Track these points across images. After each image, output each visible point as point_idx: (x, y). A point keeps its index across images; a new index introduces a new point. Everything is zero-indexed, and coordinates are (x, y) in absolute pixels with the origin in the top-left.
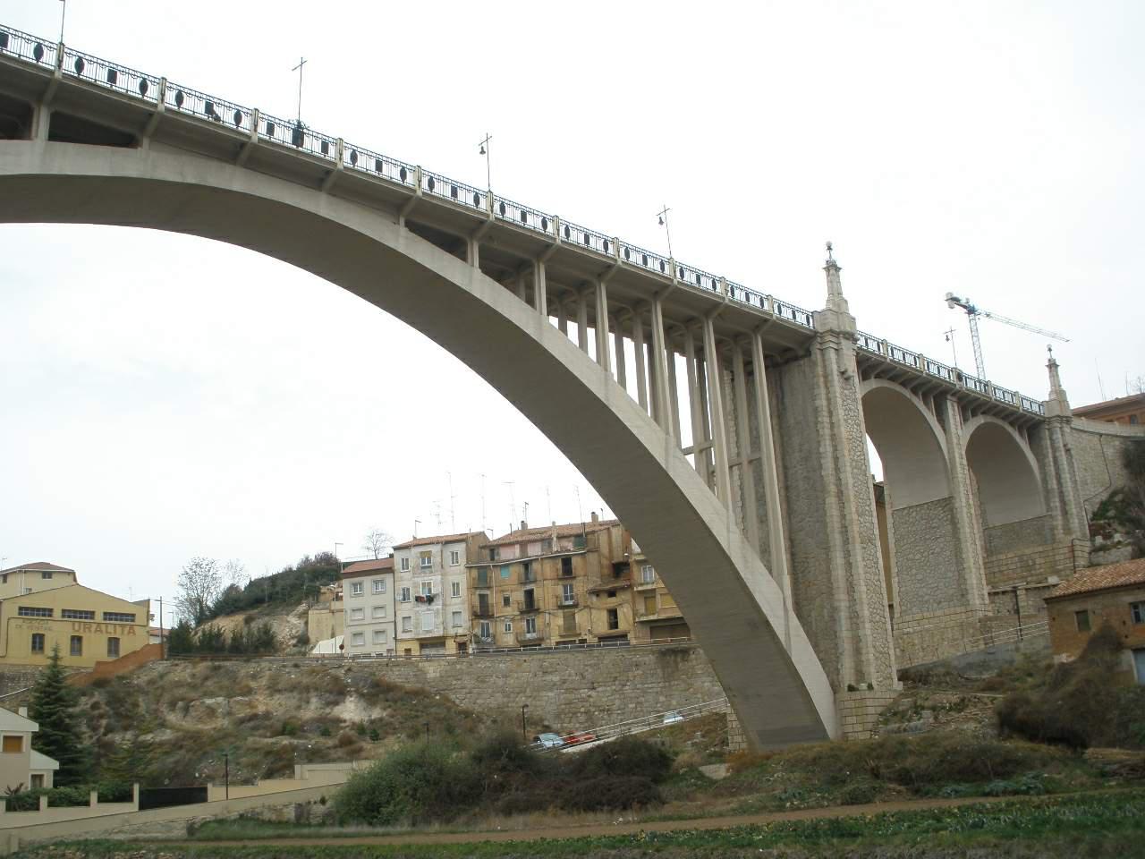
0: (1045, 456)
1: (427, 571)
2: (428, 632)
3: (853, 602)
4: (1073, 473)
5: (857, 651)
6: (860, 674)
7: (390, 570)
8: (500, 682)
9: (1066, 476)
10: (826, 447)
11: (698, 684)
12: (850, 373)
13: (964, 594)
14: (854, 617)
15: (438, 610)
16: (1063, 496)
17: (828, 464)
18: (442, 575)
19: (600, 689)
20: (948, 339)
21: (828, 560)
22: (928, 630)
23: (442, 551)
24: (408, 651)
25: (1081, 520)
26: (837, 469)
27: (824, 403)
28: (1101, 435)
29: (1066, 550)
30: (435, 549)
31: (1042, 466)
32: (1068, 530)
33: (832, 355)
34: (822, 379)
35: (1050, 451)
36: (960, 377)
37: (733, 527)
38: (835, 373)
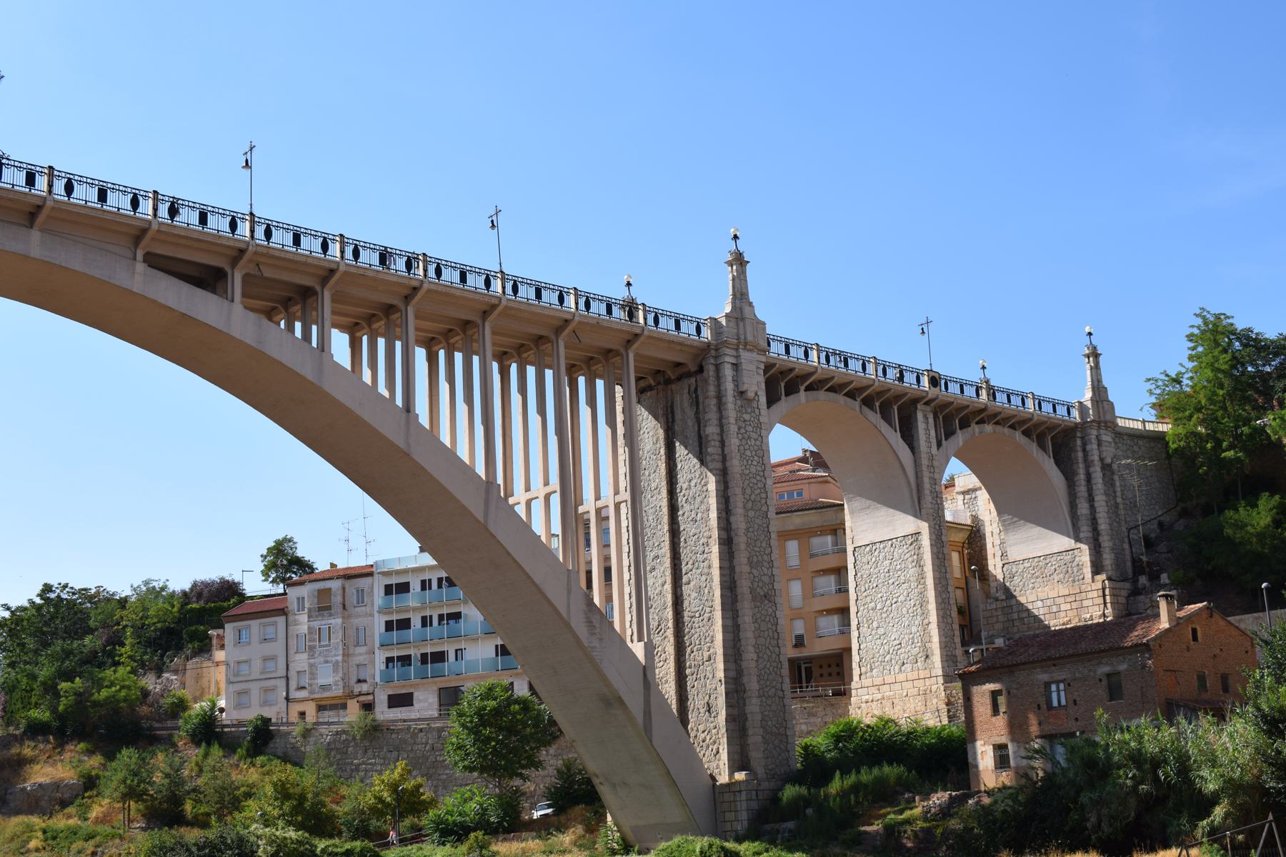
0: (1075, 473)
1: (325, 613)
7: (283, 612)
9: (1100, 499)
12: (751, 395)
15: (337, 662)
16: (1097, 523)
18: (343, 618)
20: (923, 332)
23: (344, 589)
24: (302, 714)
29: (1095, 594)
30: (335, 585)
33: (728, 372)
34: (714, 401)
35: (1081, 465)
36: (934, 381)
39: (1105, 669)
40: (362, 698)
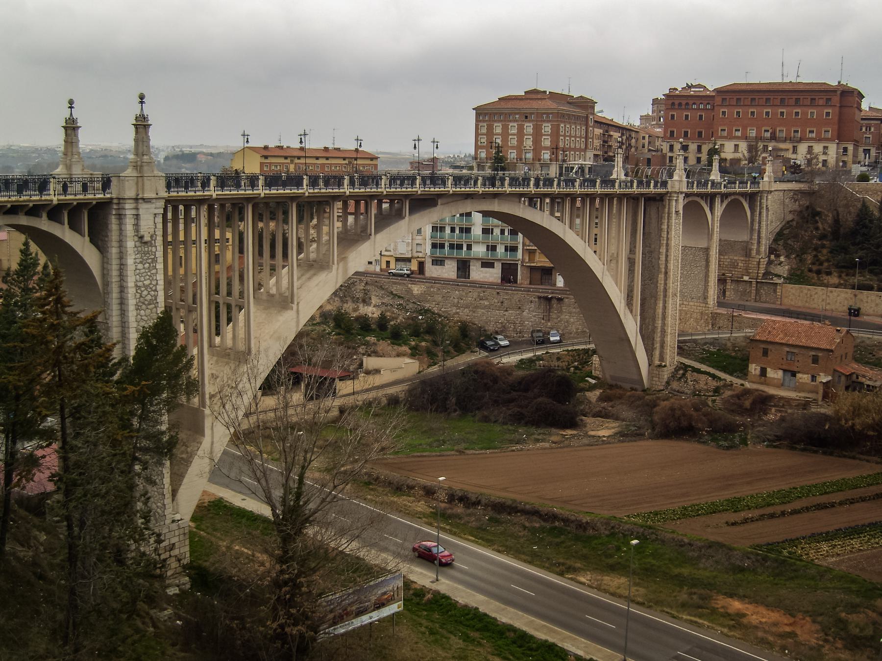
3: (664, 324)
4: (767, 216)
9: (764, 223)
10: (663, 250)
11: (562, 317)
14: (664, 332)
17: (663, 258)
21: (656, 304)
22: (685, 310)
24: (388, 263)
25: (766, 246)
26: (666, 260)
27: (666, 227)
28: (785, 191)
32: (758, 252)
33: (674, 203)
37: (623, 301)
38: (674, 212)
39: (814, 353)
40: (418, 259)
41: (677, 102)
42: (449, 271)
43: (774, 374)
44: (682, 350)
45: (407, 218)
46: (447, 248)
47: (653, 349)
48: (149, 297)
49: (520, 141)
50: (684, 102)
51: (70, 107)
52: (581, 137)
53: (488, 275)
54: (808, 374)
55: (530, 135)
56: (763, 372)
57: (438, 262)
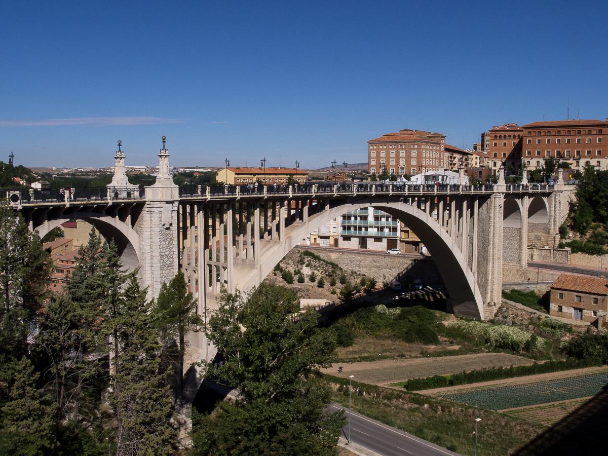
2: (324, 234)
5: (492, 292)
6: (492, 299)
8: (358, 263)
9: (557, 212)
13: (520, 260)
14: (493, 282)
19: (393, 270)
24: (315, 239)
26: (494, 236)
27: (493, 215)
31: (550, 207)
34: (493, 207)
37: (465, 263)
41: (498, 135)
42: (354, 243)
43: (568, 310)
44: (504, 294)
45: (328, 211)
46: (352, 229)
47: (486, 294)
48: (168, 262)
49: (398, 162)
50: (503, 135)
51: (118, 145)
52: (436, 159)
53: (378, 247)
54: (591, 310)
55: (403, 158)
56: (560, 308)
57: (347, 238)
